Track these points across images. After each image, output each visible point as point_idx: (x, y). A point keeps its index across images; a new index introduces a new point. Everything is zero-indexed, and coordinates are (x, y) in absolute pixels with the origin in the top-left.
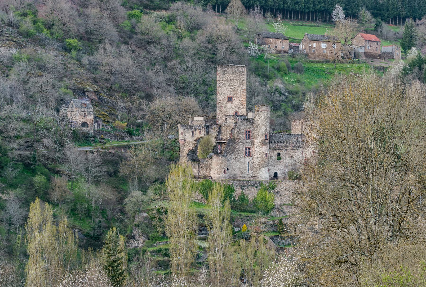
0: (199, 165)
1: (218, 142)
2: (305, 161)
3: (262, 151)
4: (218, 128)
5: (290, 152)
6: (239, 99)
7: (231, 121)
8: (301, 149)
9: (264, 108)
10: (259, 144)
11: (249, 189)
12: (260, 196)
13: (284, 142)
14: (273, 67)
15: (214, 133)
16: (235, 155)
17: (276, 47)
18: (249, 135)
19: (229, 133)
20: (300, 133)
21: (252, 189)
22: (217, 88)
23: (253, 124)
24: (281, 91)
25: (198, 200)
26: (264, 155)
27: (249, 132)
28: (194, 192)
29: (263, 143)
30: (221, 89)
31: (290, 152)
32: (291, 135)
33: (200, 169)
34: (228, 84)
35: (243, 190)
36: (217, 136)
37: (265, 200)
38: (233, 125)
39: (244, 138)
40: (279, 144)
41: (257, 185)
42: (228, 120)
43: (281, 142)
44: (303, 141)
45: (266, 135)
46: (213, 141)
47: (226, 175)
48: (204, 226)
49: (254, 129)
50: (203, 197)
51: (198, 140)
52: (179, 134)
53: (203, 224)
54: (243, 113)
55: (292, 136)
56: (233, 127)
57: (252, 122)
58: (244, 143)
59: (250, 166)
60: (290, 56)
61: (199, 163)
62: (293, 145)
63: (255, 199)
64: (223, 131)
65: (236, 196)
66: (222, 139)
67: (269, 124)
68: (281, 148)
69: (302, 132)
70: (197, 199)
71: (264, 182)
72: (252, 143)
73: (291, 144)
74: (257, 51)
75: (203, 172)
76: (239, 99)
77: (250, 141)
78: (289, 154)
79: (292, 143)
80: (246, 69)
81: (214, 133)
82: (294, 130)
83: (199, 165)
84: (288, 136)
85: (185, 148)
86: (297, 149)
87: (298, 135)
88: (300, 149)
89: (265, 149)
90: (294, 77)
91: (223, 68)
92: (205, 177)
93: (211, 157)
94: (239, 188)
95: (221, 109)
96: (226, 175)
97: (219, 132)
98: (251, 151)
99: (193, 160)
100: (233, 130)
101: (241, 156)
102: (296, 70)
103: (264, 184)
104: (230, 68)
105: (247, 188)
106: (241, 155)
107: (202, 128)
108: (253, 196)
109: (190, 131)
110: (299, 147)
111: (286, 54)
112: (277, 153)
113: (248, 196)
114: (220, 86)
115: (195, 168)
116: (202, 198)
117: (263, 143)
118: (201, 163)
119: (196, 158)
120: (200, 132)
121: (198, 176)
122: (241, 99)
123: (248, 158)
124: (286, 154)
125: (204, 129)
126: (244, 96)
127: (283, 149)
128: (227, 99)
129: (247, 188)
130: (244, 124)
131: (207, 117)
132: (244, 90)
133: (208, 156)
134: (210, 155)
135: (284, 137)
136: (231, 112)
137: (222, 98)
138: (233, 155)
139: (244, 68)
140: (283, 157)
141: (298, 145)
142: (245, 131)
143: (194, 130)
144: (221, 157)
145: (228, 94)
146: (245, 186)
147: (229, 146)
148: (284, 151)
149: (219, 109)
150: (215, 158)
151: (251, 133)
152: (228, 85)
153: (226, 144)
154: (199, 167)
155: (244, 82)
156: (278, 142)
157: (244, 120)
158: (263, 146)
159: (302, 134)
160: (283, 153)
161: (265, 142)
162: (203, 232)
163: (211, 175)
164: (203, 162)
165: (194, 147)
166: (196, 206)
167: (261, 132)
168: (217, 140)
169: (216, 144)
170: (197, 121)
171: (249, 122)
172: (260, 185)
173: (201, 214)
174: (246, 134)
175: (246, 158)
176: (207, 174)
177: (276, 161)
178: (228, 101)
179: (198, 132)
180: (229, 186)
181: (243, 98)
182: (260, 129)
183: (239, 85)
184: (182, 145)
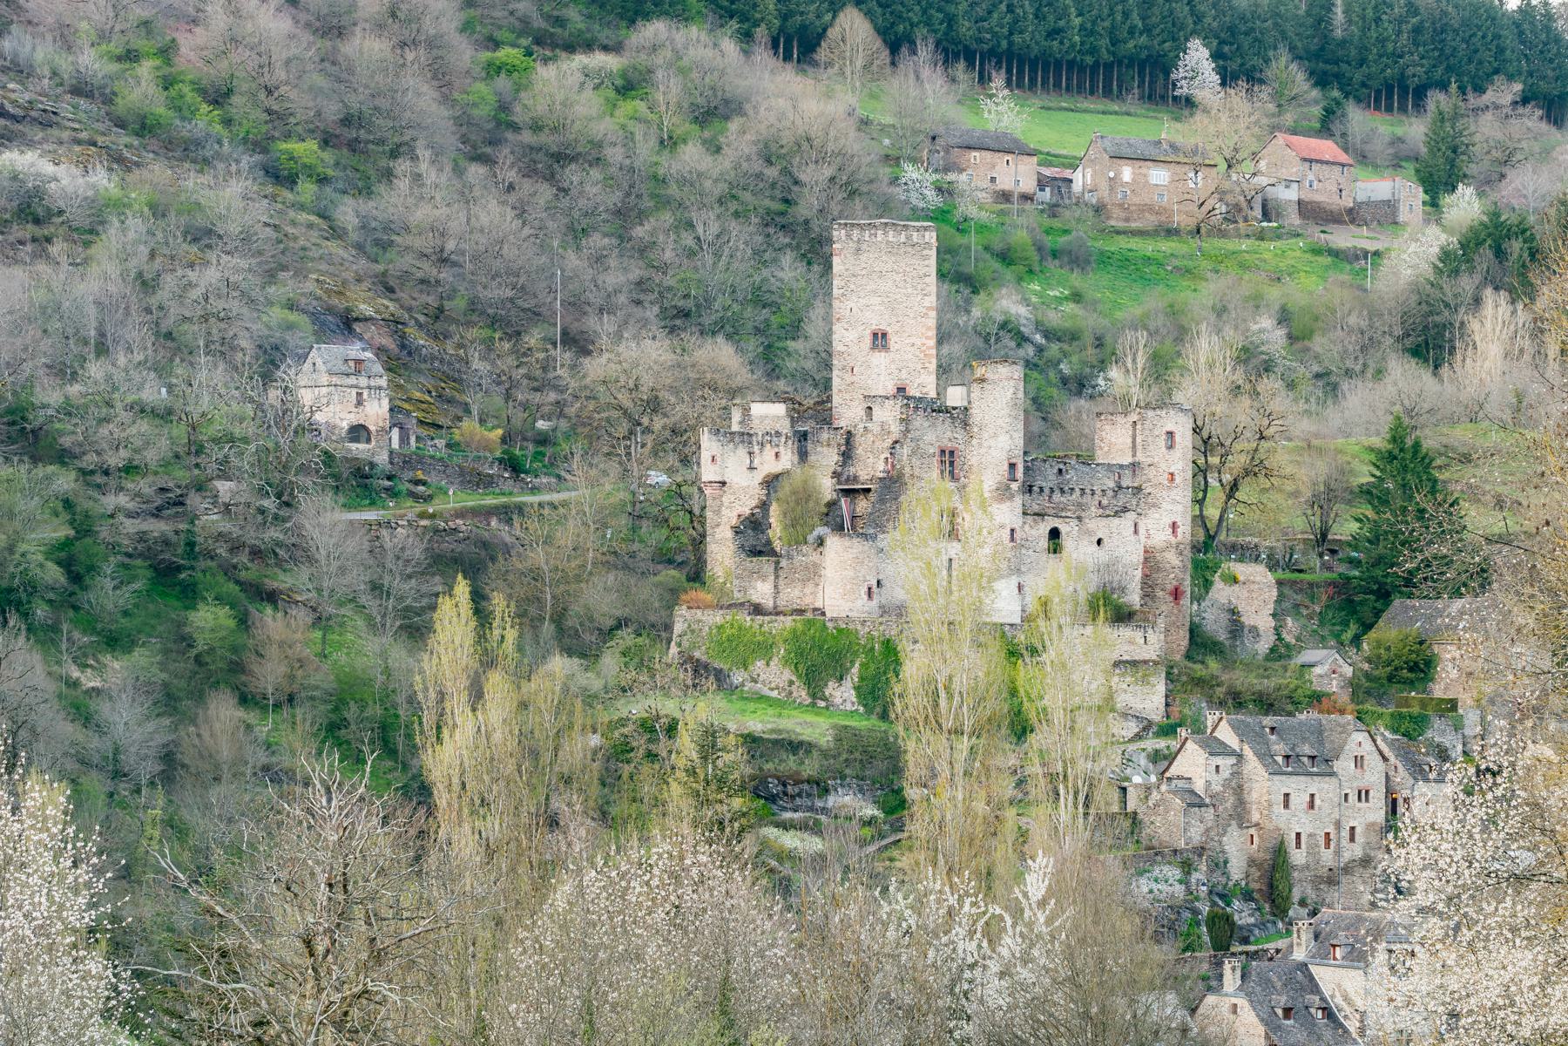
0: (776, 568)
1: (842, 490)
2: (1146, 559)
4: (843, 441)
5: (1091, 524)
6: (912, 340)
7: (888, 414)
8: (1131, 516)
9: (1003, 370)
14: (986, 248)
15: (826, 457)
17: (993, 179)
18: (952, 463)
19: (883, 457)
20: (1127, 460)
22: (836, 304)
23: (965, 424)
24: (1022, 329)
25: (776, 692)
26: (1006, 534)
27: (952, 453)
28: (763, 662)
29: (1003, 493)
30: (850, 304)
31: (1091, 524)
32: (1098, 465)
33: (781, 582)
34: (871, 286)
36: (839, 469)
38: (896, 429)
40: (1057, 497)
42: (876, 411)
43: (1062, 491)
44: (1139, 489)
45: (1012, 466)
46: (826, 487)
47: (875, 603)
48: (803, 782)
49: (968, 443)
50: (794, 678)
51: (771, 482)
52: (703, 462)
53: (798, 773)
54: (925, 390)
55: (1099, 468)
56: (895, 437)
57: (961, 418)
59: (954, 574)
60: (1042, 211)
61: (777, 563)
62: (1105, 502)
64: (860, 451)
66: (855, 479)
67: (1021, 426)
69: (1134, 456)
70: (773, 685)
71: (1007, 628)
73: (1096, 497)
74: (930, 194)
75: (793, 595)
76: (912, 340)
78: (1089, 533)
79: (1098, 492)
80: (934, 234)
81: (826, 457)
82: (1106, 449)
83: (777, 568)
84: (1086, 469)
85: (724, 511)
86: (1116, 514)
87: (1121, 466)
89: (1008, 514)
90: (1059, 283)
91: (856, 233)
92: (801, 612)
93: (821, 542)
95: (848, 378)
96: (875, 603)
97: (847, 455)
98: (959, 520)
99: (756, 553)
100: (898, 446)
102: (1066, 259)
103: (1009, 634)
104: (879, 232)
107: (783, 440)
109: (742, 452)
110: (1125, 510)
111: (1028, 206)
114: (843, 295)
115: (764, 578)
116: (791, 683)
117: (1003, 493)
118: (784, 563)
119: (765, 545)
120: (777, 455)
121: (775, 607)
122: (918, 342)
125: (790, 442)
126: (929, 328)
127: (1069, 514)
128: (868, 340)
131: (796, 406)
132: (929, 308)
133: (811, 538)
134: (815, 533)
135: (1072, 472)
136: (885, 387)
137: (851, 336)
139: (927, 234)
140: (1067, 542)
141: (1122, 499)
142: (938, 452)
143: (756, 448)
144: (855, 540)
145: (874, 322)
147: (882, 501)
148: (1074, 522)
149: (840, 373)
150: (834, 543)
152: (874, 292)
153: (873, 496)
154: (777, 577)
155: (927, 280)
156: (1052, 490)
157: (933, 411)
159: (1133, 464)
160: (1069, 529)
161: (1008, 488)
162: (798, 801)
163: (819, 604)
164: (790, 557)
165: (757, 507)
166: (771, 711)
167: (994, 452)
168: (839, 483)
169: (835, 496)
170: (763, 418)
171: (952, 417)
173: (793, 737)
176: (807, 600)
177: (1045, 556)
178: (874, 347)
179: (769, 452)
180: (888, 641)
181: (927, 338)
182: (992, 442)
183: (910, 290)
184: (714, 499)
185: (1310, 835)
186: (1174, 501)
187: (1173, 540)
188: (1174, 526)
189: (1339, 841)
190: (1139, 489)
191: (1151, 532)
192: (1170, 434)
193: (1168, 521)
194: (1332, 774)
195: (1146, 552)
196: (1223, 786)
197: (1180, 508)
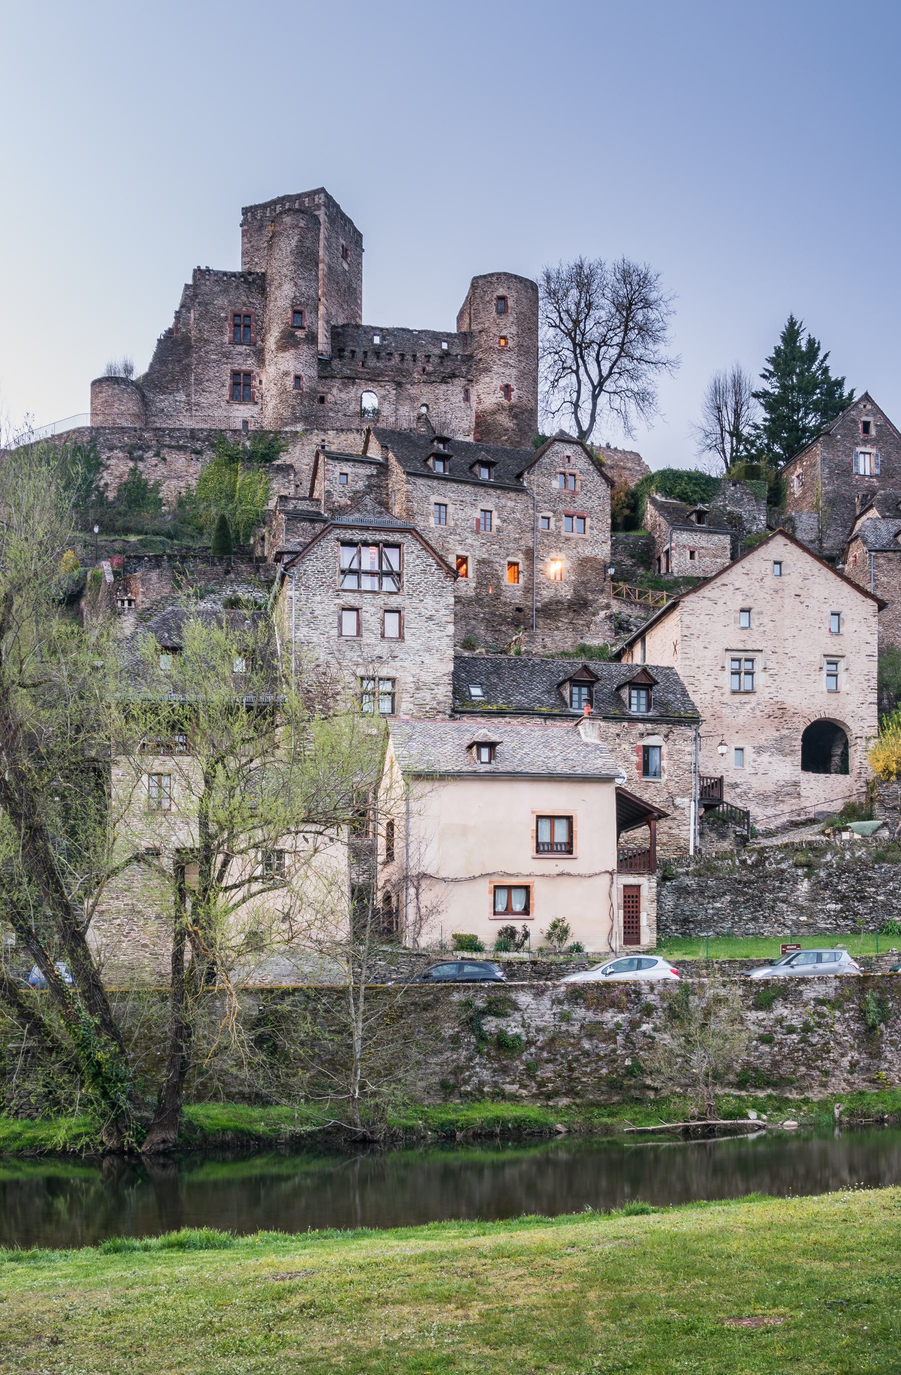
3: (283, 368)
5: (413, 391)
10: (273, 347)
11: (164, 459)
12: (210, 485)
13: (390, 354)
16: (188, 395)
21: (179, 461)
26: (290, 382)
35: (141, 465)
37: (230, 497)
39: (226, 339)
40: (372, 362)
41: (198, 445)
58: (227, 355)
62: (430, 368)
63: (189, 496)
65: (106, 485)
68: (379, 375)
71: (229, 434)
72: (260, 355)
77: (252, 348)
79: (424, 360)
86: (444, 381)
88: (456, 381)
94: (121, 455)
98: (255, 383)
101: (212, 398)
105: (157, 455)
106: (215, 395)
108: (182, 484)
110: (453, 376)
113: (158, 484)
123: (241, 407)
124: (398, 396)
129: (157, 455)
130: (225, 291)
138: (181, 397)
146: (149, 448)
151: (256, 322)
156: (365, 353)
158: (284, 351)
172: (213, 445)
175: (236, 407)
185: (482, 562)
186: (506, 365)
187: (505, 402)
188: (507, 389)
189: (532, 574)
190: (471, 357)
191: (482, 397)
192: (502, 298)
193: (498, 383)
194: (521, 490)
195: (477, 417)
196: (352, 499)
197: (514, 372)
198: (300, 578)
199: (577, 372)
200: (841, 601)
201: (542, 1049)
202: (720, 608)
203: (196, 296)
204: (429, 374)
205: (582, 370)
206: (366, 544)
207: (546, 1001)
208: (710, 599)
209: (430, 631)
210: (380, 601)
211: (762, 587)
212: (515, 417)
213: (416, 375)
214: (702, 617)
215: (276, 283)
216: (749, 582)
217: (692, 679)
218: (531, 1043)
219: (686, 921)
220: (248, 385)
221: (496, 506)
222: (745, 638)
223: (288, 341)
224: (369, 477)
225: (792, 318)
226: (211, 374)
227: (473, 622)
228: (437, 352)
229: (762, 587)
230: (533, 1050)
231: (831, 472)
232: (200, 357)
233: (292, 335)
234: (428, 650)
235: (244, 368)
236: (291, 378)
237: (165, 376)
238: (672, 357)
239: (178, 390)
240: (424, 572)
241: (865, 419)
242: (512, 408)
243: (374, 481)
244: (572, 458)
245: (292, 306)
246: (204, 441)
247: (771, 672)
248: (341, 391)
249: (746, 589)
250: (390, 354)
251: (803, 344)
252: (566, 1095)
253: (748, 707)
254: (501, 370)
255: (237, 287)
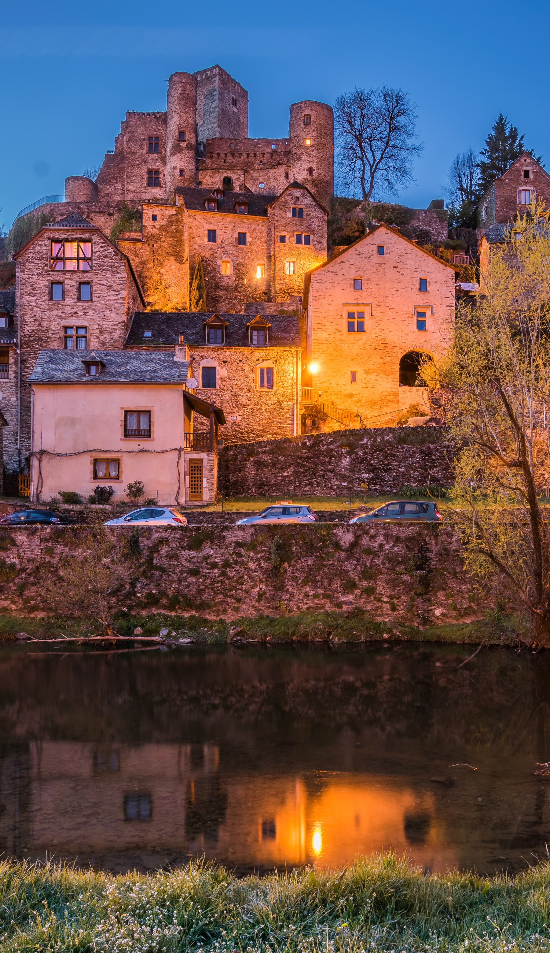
3: (173, 165)
5: (255, 174)
16: (123, 185)
26: (177, 173)
39: (144, 151)
40: (230, 159)
43: (233, 155)
58: (145, 161)
68: (234, 167)
77: (159, 155)
86: (273, 167)
98: (161, 176)
101: (137, 186)
106: (138, 184)
110: (279, 164)
112: (222, 177)
123: (153, 190)
138: (119, 186)
141: (276, 158)
151: (161, 140)
156: (226, 155)
174: (150, 144)
175: (150, 190)
186: (310, 155)
188: (311, 170)
190: (290, 152)
193: (305, 166)
196: (159, 230)
197: (315, 159)
198: (24, 264)
199: (362, 159)
200: (427, 270)
201: (30, 574)
202: (340, 277)
203: (127, 127)
204: (264, 164)
205: (364, 157)
206: (67, 240)
207: (36, 540)
208: (332, 272)
209: (110, 295)
210: (76, 277)
211: (369, 262)
212: (316, 186)
213: (256, 165)
214: (326, 284)
215: (170, 116)
216: (360, 260)
217: (320, 326)
218: (23, 570)
219: (262, 485)
220: (157, 178)
221: (249, 230)
222: (358, 297)
223: (177, 149)
224: (171, 216)
225: (501, 116)
226: (136, 172)
227: (233, 302)
228: (269, 150)
229: (369, 262)
230: (23, 575)
231: (501, 204)
232: (129, 162)
233: (178, 146)
234: (109, 307)
235: (155, 167)
236: (178, 170)
237: (109, 175)
238: (418, 144)
239: (117, 183)
240: (106, 257)
241: (525, 168)
242: (313, 181)
243: (174, 218)
244: (301, 199)
245: (178, 129)
246: (114, 208)
247: (377, 319)
248: (211, 177)
249: (358, 264)
250: (241, 154)
251: (507, 132)
252: (43, 609)
253: (360, 343)
254: (307, 159)
255: (151, 121)
